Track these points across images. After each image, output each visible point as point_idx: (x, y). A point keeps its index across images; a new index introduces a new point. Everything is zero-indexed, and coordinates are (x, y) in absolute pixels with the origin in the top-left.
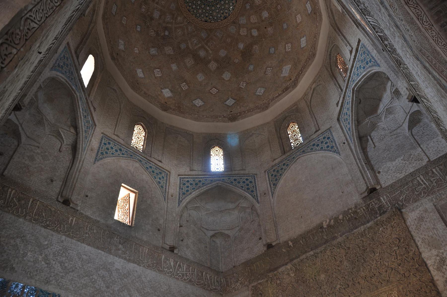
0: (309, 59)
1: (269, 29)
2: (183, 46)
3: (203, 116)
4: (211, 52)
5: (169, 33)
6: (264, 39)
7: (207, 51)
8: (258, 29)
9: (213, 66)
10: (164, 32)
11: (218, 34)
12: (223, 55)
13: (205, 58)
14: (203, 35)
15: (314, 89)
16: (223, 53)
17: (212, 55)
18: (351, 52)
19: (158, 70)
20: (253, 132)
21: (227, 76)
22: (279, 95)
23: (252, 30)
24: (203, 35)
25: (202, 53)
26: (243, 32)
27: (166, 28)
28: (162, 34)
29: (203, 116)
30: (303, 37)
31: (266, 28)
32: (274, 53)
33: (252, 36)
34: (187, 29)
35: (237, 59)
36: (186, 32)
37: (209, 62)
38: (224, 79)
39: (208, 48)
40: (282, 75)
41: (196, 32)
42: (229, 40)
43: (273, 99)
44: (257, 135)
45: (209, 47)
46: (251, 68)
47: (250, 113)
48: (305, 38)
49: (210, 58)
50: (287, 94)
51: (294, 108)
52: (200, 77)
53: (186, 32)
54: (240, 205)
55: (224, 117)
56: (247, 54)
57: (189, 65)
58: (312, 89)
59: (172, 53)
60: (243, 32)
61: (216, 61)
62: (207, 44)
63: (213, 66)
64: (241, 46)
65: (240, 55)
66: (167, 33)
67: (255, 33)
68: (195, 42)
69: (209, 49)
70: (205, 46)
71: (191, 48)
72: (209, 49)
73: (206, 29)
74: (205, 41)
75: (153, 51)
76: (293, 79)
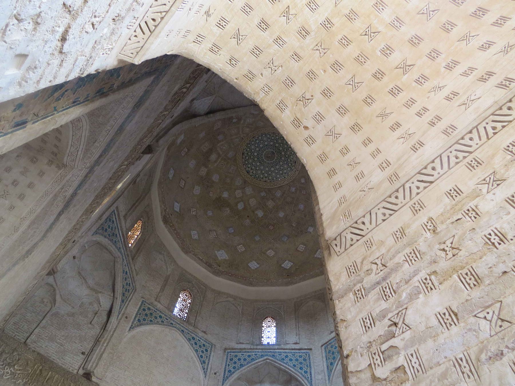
0: (246, 280)
1: (248, 220)
2: (221, 137)
3: (163, 188)
4: (216, 164)
7: (215, 162)
8: (245, 209)
9: (203, 171)
12: (214, 178)
13: (209, 161)
14: (231, 154)
15: (228, 301)
16: (215, 178)
18: (296, 343)
20: (165, 254)
21: (197, 190)
22: (202, 260)
25: (213, 157)
26: (238, 193)
29: (163, 188)
30: (258, 264)
32: (230, 234)
37: (206, 167)
38: (194, 188)
40: (216, 252)
41: (233, 146)
42: (228, 180)
43: (195, 255)
44: (163, 260)
46: (210, 213)
47: (175, 236)
48: (258, 266)
49: (210, 166)
50: (205, 268)
51: (202, 287)
52: (192, 164)
54: (100, 295)
55: (165, 210)
56: (220, 203)
58: (227, 299)
59: (215, 129)
60: (238, 193)
63: (203, 171)
64: (225, 195)
67: (240, 206)
76: (221, 268)
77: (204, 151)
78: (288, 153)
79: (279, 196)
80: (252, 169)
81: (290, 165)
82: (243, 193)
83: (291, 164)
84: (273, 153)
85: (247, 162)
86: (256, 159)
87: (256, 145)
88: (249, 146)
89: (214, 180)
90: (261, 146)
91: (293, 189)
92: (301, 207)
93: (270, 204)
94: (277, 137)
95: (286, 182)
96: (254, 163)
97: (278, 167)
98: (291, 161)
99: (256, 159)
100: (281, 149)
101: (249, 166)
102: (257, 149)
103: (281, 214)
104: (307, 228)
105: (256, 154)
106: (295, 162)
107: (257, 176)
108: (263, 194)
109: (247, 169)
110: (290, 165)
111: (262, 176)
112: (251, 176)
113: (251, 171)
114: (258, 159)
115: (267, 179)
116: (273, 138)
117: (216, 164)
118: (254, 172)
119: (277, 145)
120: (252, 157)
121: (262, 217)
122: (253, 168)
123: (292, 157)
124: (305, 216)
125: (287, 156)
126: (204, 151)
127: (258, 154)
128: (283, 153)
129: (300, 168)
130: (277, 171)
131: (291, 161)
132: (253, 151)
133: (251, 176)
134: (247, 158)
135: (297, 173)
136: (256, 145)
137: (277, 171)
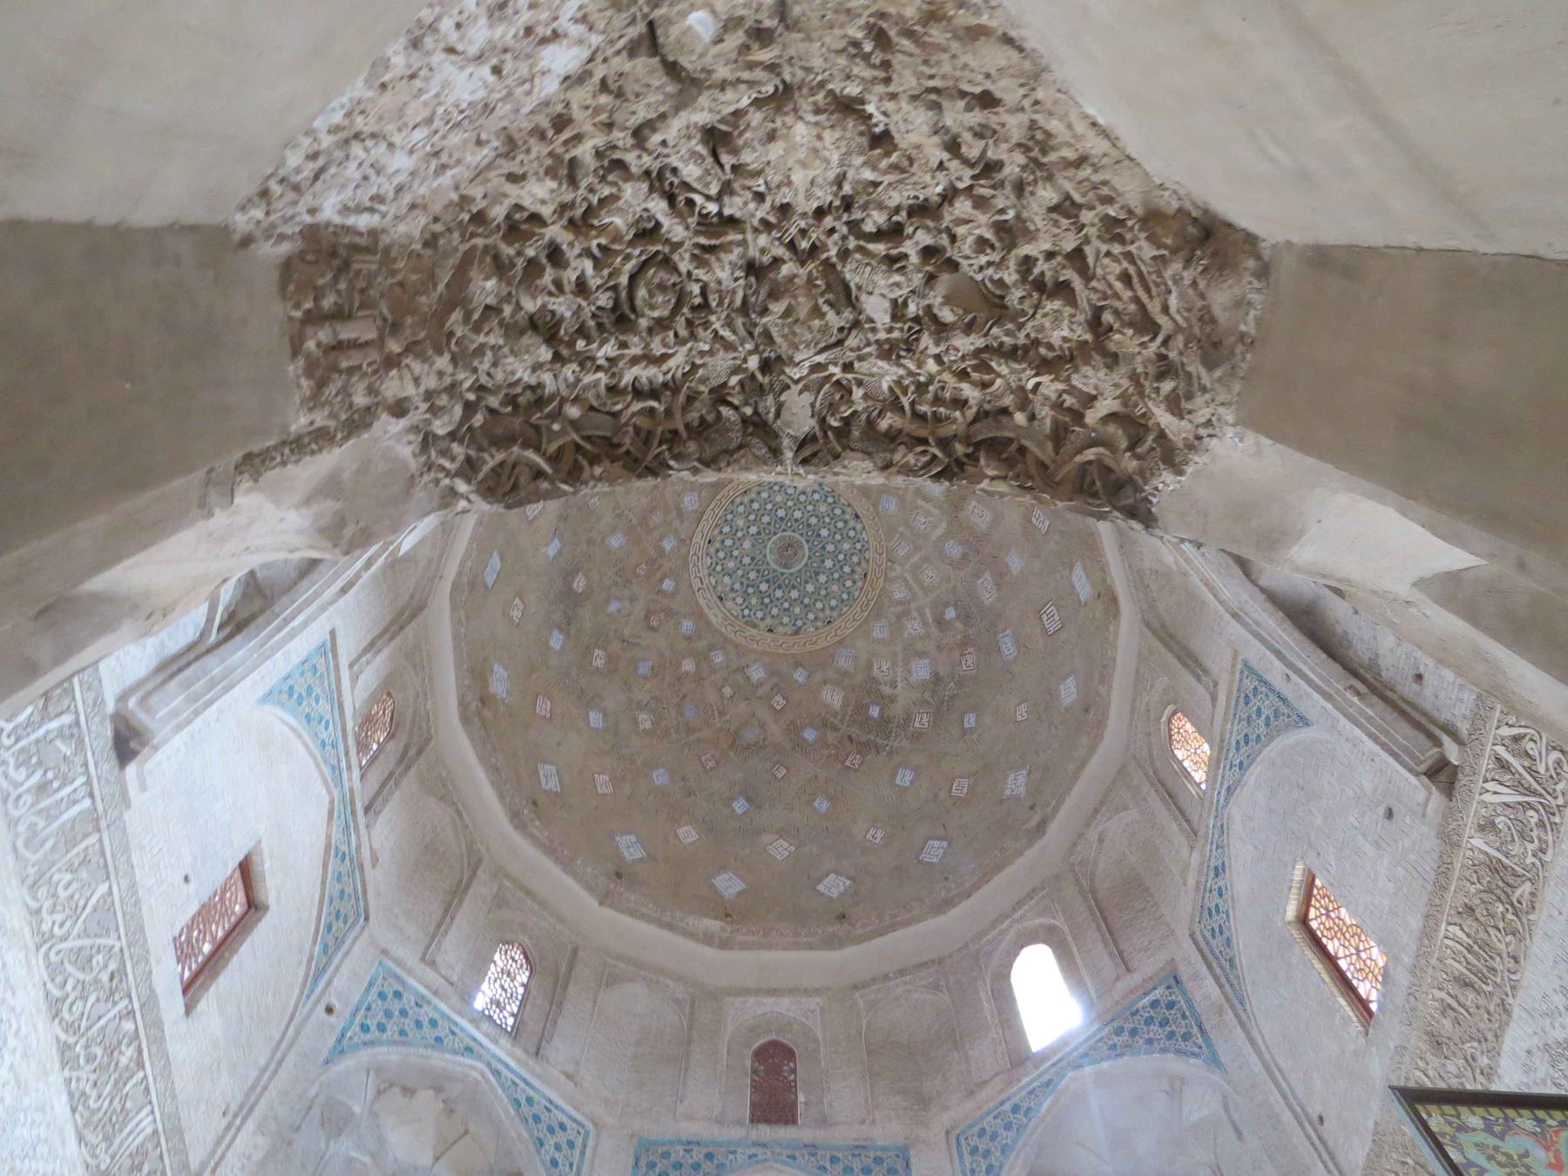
2: (954, 550)
5: (947, 605)
10: (949, 622)
19: (1045, 617)
27: (940, 622)
28: (958, 625)
34: (908, 557)
57: (988, 516)
66: (950, 613)
71: (944, 524)
73: (875, 506)
75: (1008, 648)
77: (974, 503)
78: (754, 601)
79: (686, 500)
87: (841, 557)
88: (858, 546)
90: (829, 563)
91: (668, 545)
92: (616, 541)
94: (811, 616)
95: (697, 538)
99: (813, 521)
100: (779, 593)
101: (816, 496)
102: (830, 548)
104: (561, 537)
105: (824, 532)
106: (721, 599)
114: (809, 525)
115: (746, 500)
116: (819, 605)
120: (827, 520)
123: (740, 600)
124: (589, 542)
125: (750, 590)
126: (974, 503)
127: (819, 535)
128: (764, 587)
129: (702, 602)
134: (838, 512)
135: (696, 584)
137: (739, 534)
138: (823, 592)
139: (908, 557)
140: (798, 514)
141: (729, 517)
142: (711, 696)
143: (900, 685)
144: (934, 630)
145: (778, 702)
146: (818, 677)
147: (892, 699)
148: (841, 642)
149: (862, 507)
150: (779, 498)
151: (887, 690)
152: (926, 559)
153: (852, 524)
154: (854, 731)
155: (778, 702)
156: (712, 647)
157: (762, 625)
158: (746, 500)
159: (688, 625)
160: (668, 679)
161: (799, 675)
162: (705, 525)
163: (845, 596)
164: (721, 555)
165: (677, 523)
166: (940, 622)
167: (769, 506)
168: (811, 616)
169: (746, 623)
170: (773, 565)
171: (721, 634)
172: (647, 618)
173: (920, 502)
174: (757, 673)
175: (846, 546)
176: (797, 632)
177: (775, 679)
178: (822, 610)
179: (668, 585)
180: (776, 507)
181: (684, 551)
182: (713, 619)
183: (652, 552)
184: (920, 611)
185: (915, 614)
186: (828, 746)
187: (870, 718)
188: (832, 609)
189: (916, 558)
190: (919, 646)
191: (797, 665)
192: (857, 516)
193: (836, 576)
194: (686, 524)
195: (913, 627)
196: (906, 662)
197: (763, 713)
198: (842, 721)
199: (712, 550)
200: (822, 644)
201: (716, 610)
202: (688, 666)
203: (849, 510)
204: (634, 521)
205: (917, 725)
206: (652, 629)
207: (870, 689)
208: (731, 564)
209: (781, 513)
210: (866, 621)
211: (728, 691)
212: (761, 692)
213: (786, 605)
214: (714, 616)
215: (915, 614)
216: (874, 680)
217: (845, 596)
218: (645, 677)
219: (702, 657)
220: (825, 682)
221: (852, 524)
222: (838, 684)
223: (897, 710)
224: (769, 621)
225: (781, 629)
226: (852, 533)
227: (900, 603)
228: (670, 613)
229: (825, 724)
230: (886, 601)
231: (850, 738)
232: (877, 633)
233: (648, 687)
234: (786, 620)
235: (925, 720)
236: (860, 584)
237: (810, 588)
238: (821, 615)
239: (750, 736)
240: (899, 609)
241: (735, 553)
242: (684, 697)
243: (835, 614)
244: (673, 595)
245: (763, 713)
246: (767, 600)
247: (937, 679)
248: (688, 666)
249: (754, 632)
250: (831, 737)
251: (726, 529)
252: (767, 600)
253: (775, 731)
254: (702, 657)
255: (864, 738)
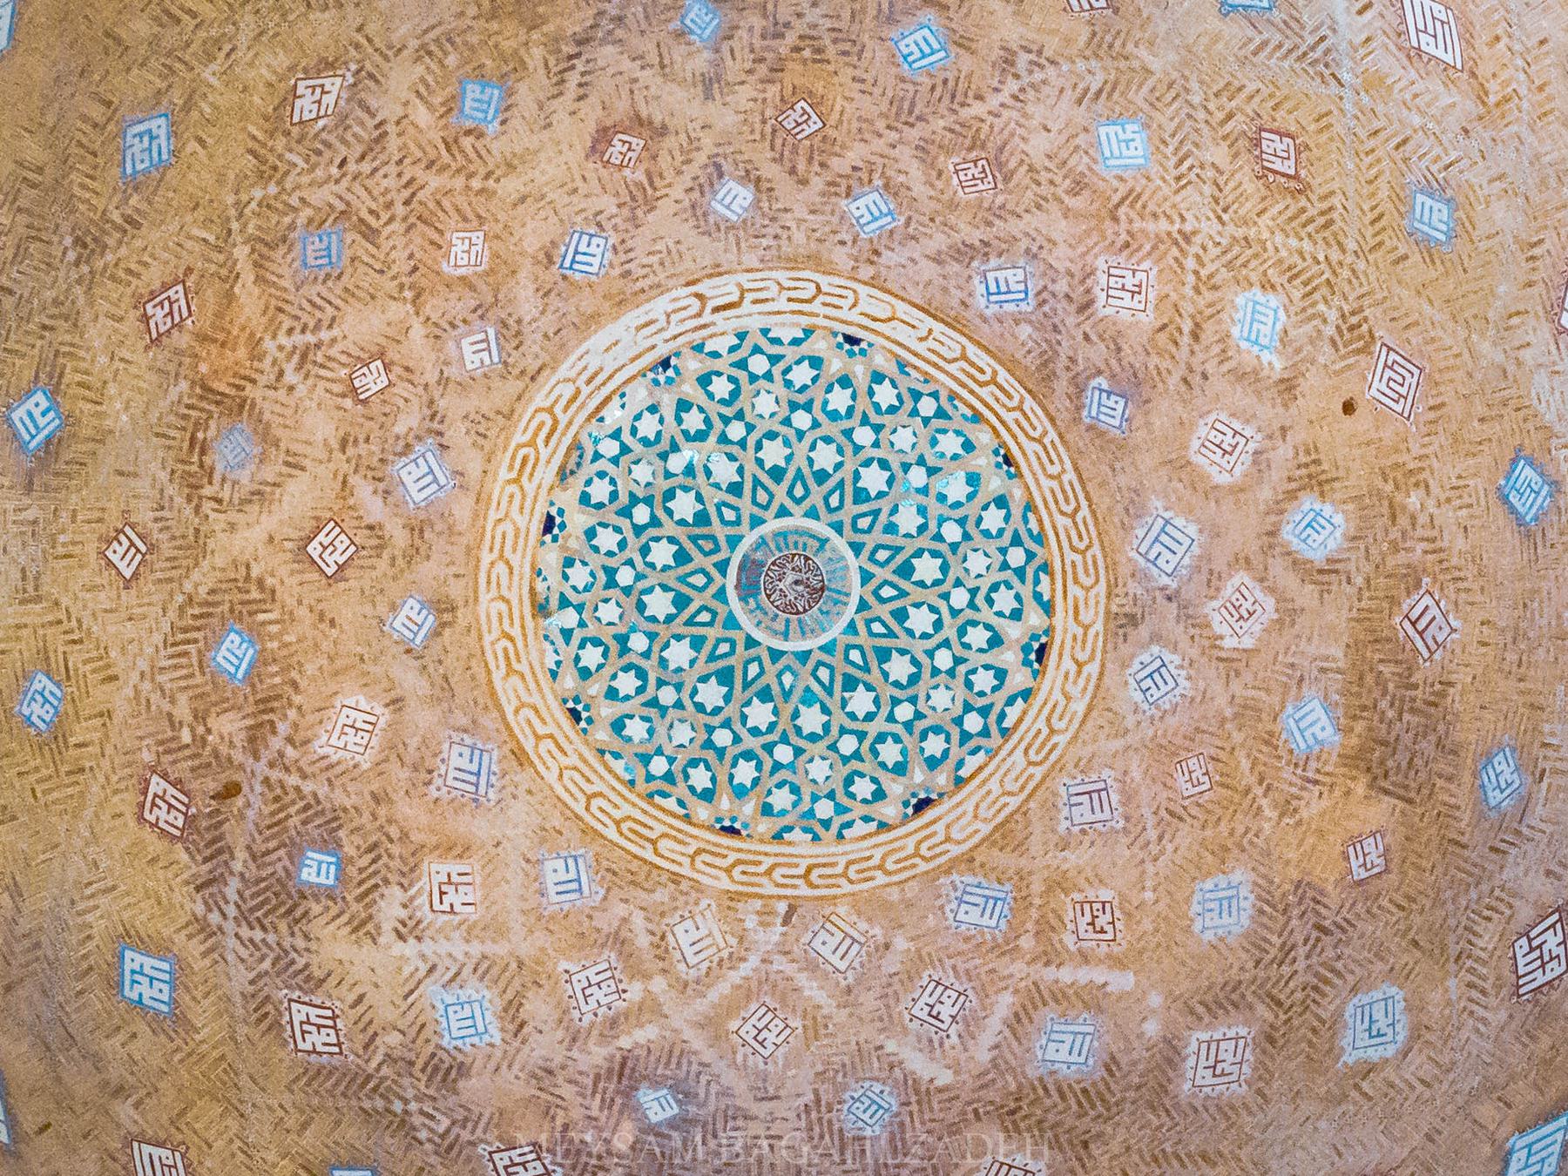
4: (1120, 981)
6: (1414, 500)
7: (1093, 1000)
11: (1083, 814)
17: (1155, 1000)
23: (1287, 534)
24: (974, 916)
25: (1064, 1050)
31: (1348, 408)
33: (1325, 574)
34: (812, 966)
35: (1356, 840)
36: (820, 997)
37: (1170, 1054)
39: (1084, 975)
41: (901, 943)
45: (1085, 958)
49: (1152, 1028)
53: (820, 997)
61: (1222, 1001)
62: (1049, 957)
64: (1314, 724)
65: (1360, 789)
68: (946, 1011)
69: (1098, 975)
70: (1050, 974)
71: (945, 1078)
72: (1098, 975)
74: (1026, 942)
78: (642, 473)
79: (1014, 277)
80: (996, 641)
81: (721, 387)
82: (1213, 582)
83: (704, 381)
84: (750, 567)
85: (973, 723)
86: (899, 668)
87: (783, 753)
89: (1248, 902)
90: (760, 714)
93: (1129, 299)
94: (592, 656)
95: (873, 303)
96: (944, 659)
97: (825, 457)
98: (683, 406)
99: (899, 668)
100: (662, 554)
101: (984, 680)
103: (1124, 147)
105: (861, 702)
107: (1016, 557)
108: (1108, 410)
109: (1019, 678)
110: (721, 387)
111: (993, 519)
112: (1048, 608)
113: (1013, 632)
114: (884, 655)
116: (627, 683)
117: (1120, 981)
118: (1005, 601)
119: (660, 604)
120: (904, 712)
121: (1268, 286)
122: (977, 637)
123: (648, 426)
129: (658, 307)
130: (864, 436)
131: (683, 406)
132: (848, 745)
133: (1048, 608)
134: (934, 745)
135: (722, 289)
136: (783, 753)
137: (864, 436)
138: (667, 696)
139: (812, 966)
140: (920, 620)
141: (927, 407)
142: (360, 326)
143: (410, 948)
144: (596, 1055)
145: (332, 549)
146: (410, 680)
147: (363, 927)
148: (520, 756)
149: (963, 820)
150: (977, 563)
151: (390, 908)
152: (815, 1027)
153: (896, 788)
154: (254, 804)
155: (332, 549)
156: (511, 332)
157: (568, 498)
158: (983, 461)
159: (595, 254)
160: (434, 181)
161: (411, 620)
162: (914, 333)
163: (659, 766)
164: (802, 374)
165: (939, 241)
166: (625, 1075)
167: (952, 532)
168: (592, 656)
169: (576, 446)
170: (750, 539)
171: (554, 364)
172: (639, 123)
173: (1005, 1003)
174: (417, 478)
175: (819, 770)
176: (541, 609)
177: (399, 537)
178: (612, 694)
179: (734, 199)
180: (947, 556)
181: (841, 257)
182: (599, 339)
183: (856, 154)
184: (649, 1009)
185: (635, 991)
186: (200, 717)
187: (296, 854)
188: (618, 726)
189: (813, 990)
190: (537, 1007)
191: (443, 608)
192: (922, 805)
193: (722, 738)
194: (928, 270)
195: (592, 986)
196: (484, 969)
197: (300, 497)
198: (279, 761)
199: (819, 345)
200: (508, 690)
201: (622, 354)
202: (465, 252)
203: (942, 779)
204: (977, 109)
205: (299, 1013)
206: (603, 136)
207: (381, 864)
208: (765, 404)
209: (927, 568)
210: (589, 833)
211: (373, 380)
212: (364, 490)
213: (625, 577)
214: (617, 343)
215: (635, 991)
216: (409, 874)
217: (659, 766)
218: (451, 106)
219: (486, 299)
220: (396, 703)
221: (896, 788)
222: (393, 748)
223: (332, 945)
224: (578, 520)
225: (551, 557)
226: (863, 788)
227: (661, 946)
228: (641, 200)
229: (266, 704)
230: (661, 896)
231: (231, 790)
232: (555, 871)
233: (422, 115)
234: (579, 576)
235: (316, 1039)
236: (703, 812)
237: (679, 654)
238: (595, 688)
239: (231, 451)
240: (643, 941)
241: (802, 420)
242: (370, 234)
243: (602, 735)
244: (698, 213)
245: (300, 497)
246: (641, 514)
247: (447, 1072)
248: (465, 252)
249: (548, 474)
250: (228, 726)
251: (885, 395)
252: (641, 514)
253: (246, 539)
254: (486, 299)
255: (238, 836)
